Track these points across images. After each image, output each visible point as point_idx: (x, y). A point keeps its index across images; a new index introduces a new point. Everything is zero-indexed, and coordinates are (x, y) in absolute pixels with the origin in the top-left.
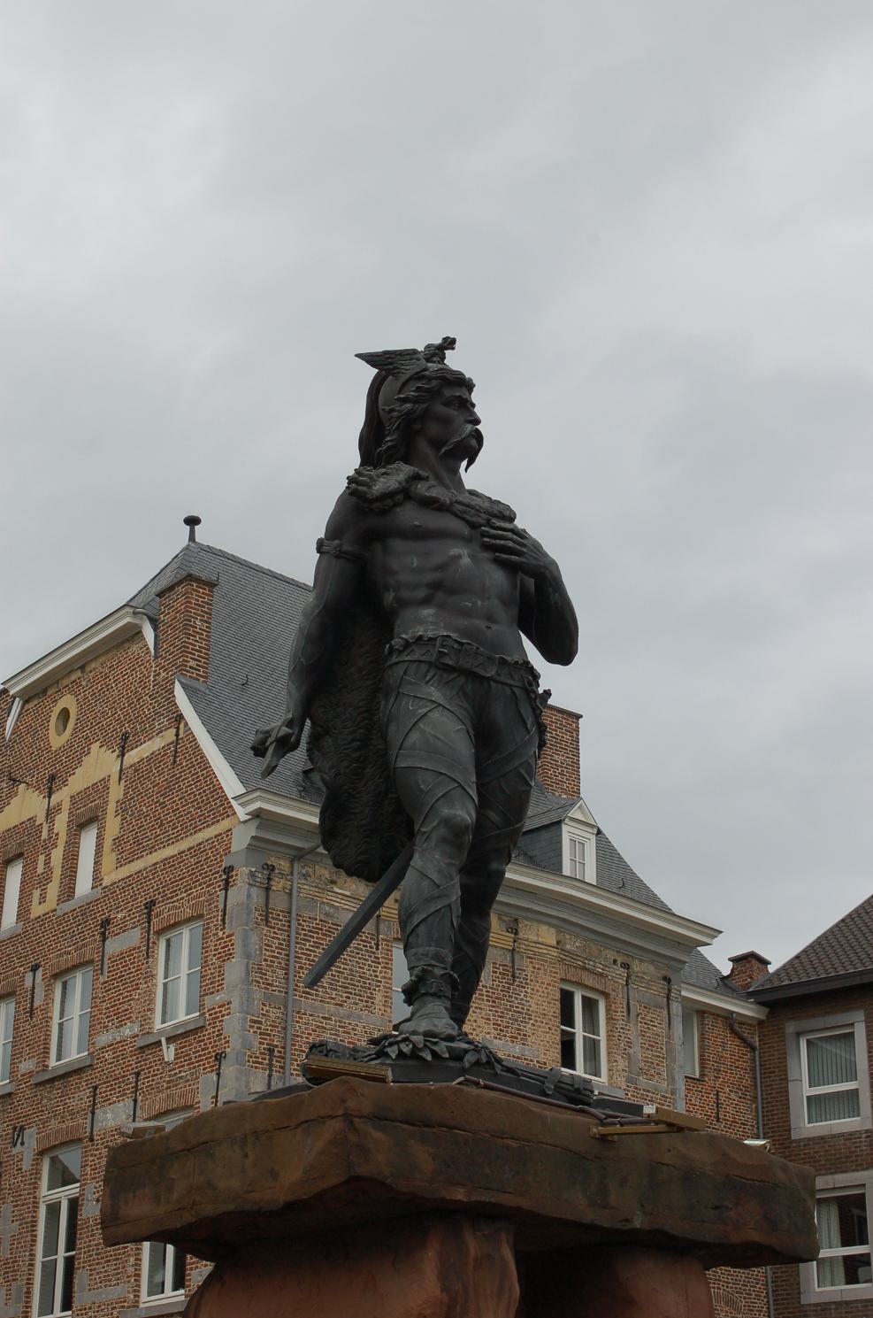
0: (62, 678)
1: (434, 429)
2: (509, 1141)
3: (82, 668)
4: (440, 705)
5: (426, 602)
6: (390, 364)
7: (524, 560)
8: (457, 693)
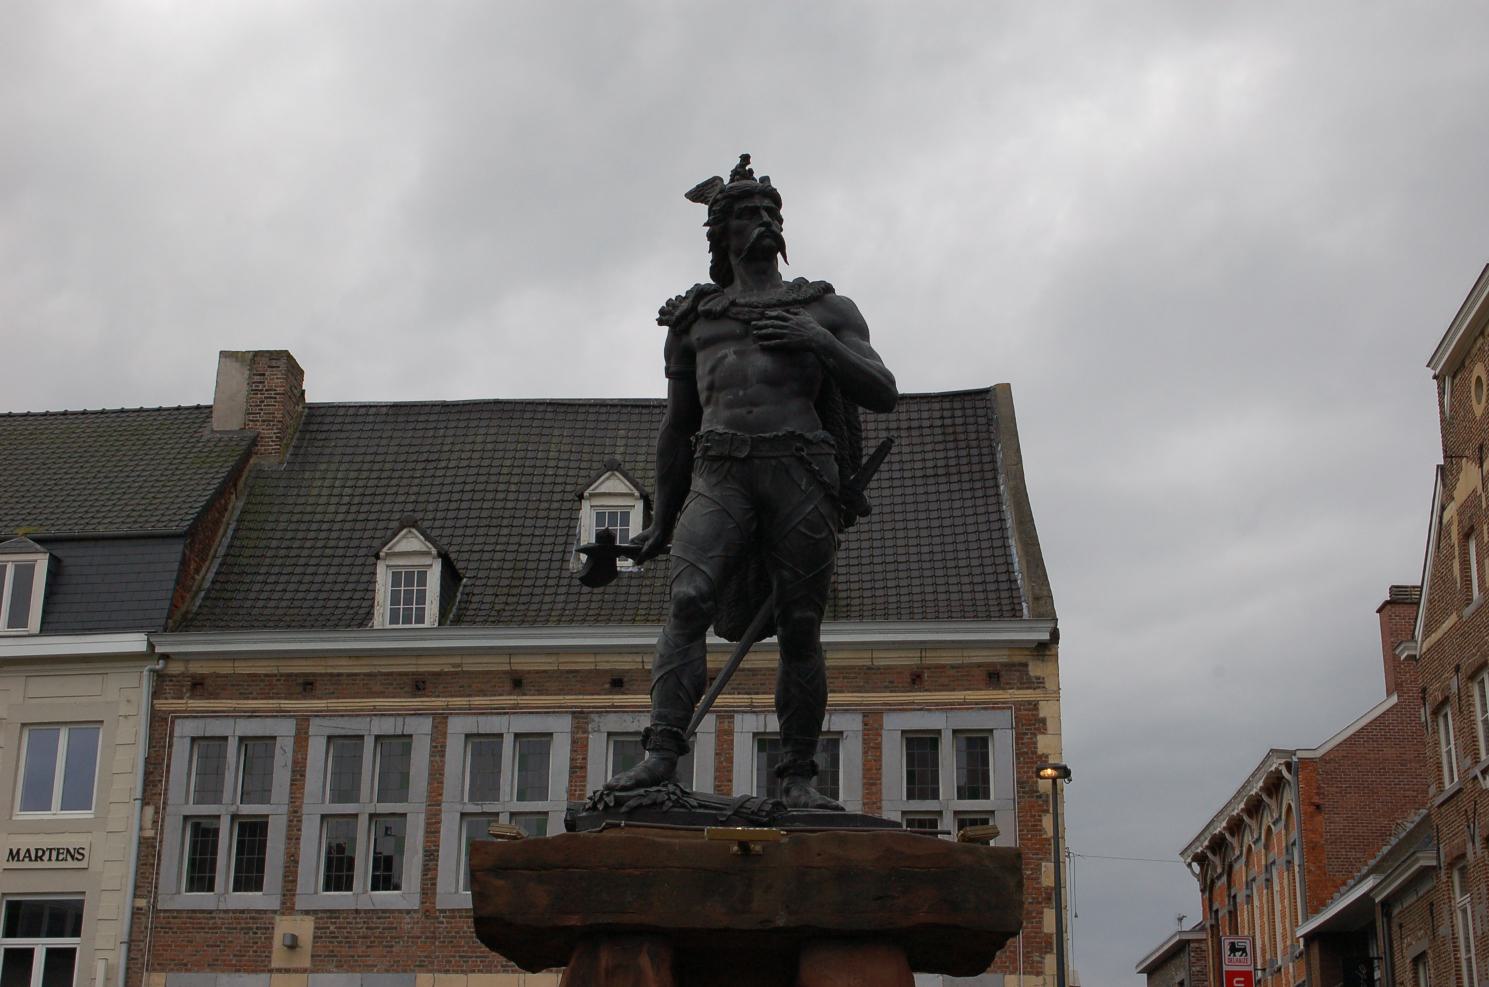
0: (1472, 347)
1: (734, 243)
2: (631, 870)
3: (1482, 333)
4: (700, 494)
5: (708, 401)
6: (702, 195)
7: (785, 340)
8: (725, 477)
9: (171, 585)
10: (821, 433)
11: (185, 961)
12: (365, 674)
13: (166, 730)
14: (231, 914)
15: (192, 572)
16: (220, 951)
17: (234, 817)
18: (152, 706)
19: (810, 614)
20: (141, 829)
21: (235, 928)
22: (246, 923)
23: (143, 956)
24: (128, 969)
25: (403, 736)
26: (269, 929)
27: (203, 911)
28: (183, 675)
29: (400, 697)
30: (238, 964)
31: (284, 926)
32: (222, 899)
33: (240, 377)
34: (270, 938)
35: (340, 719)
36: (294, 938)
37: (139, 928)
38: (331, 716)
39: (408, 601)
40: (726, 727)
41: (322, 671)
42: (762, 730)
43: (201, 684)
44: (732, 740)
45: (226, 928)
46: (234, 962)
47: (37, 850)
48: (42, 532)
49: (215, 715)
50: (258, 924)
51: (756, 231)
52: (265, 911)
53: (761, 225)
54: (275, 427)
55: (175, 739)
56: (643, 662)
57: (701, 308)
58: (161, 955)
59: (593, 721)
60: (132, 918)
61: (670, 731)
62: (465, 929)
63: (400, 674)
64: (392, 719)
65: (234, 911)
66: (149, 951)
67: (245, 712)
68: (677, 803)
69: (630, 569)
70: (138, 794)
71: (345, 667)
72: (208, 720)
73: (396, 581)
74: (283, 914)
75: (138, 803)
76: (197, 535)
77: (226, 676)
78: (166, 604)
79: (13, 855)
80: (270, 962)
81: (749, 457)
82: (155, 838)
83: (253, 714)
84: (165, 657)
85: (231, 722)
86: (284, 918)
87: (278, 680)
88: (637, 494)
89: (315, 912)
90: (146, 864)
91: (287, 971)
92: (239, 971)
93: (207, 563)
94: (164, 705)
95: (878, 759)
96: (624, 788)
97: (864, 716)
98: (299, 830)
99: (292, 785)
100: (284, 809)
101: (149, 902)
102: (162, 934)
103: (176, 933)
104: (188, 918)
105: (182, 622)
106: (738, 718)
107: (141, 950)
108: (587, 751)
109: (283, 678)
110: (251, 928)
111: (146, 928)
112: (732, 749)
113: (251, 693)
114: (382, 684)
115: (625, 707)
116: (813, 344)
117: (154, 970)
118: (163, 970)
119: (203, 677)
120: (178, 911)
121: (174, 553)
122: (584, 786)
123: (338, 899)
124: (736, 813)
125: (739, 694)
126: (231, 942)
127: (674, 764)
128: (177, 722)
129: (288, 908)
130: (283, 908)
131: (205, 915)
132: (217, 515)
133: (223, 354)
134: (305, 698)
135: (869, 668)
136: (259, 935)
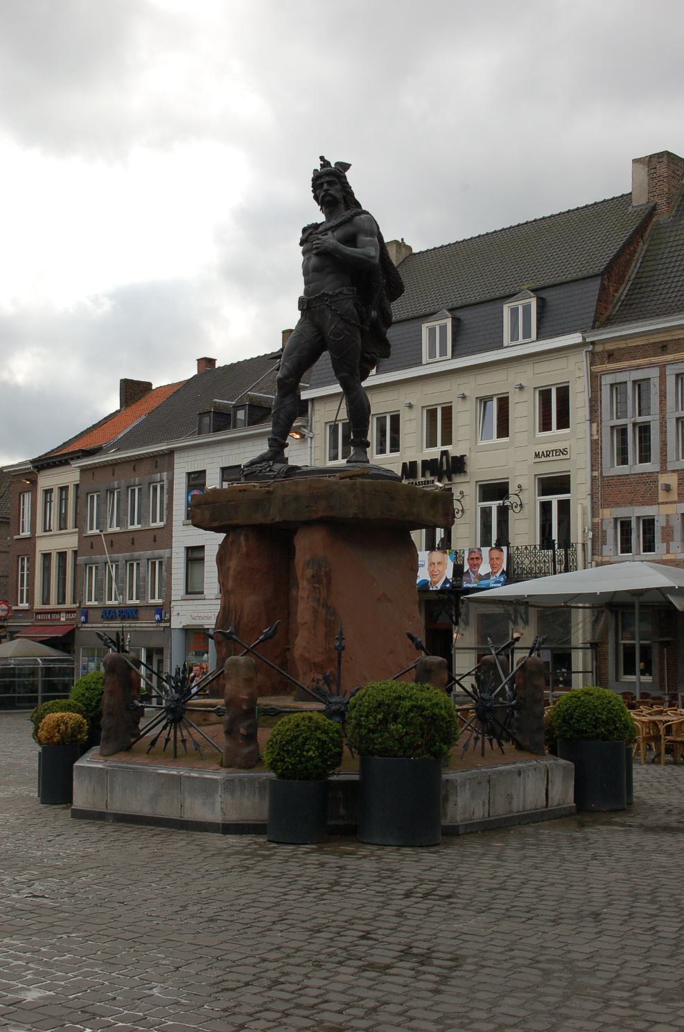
9: (595, 303)
15: (612, 293)
17: (634, 424)
20: (591, 435)
24: (592, 508)
27: (624, 475)
28: (603, 351)
33: (643, 171)
41: (670, 338)
47: (547, 451)
48: (534, 286)
49: (621, 370)
50: (650, 478)
52: (653, 473)
55: (603, 386)
60: (592, 484)
65: (639, 474)
70: (588, 418)
74: (662, 473)
75: (588, 422)
76: (613, 271)
77: (623, 349)
79: (537, 455)
83: (638, 368)
84: (593, 343)
85: (628, 373)
86: (663, 475)
89: (677, 471)
90: (595, 454)
91: (667, 503)
92: (643, 505)
93: (624, 285)
98: (666, 427)
99: (660, 404)
100: (657, 417)
105: (602, 320)
118: (608, 508)
120: (613, 476)
121: (595, 285)
124: (278, 473)
128: (603, 377)
129: (664, 470)
132: (628, 257)
133: (635, 161)
134: (663, 355)
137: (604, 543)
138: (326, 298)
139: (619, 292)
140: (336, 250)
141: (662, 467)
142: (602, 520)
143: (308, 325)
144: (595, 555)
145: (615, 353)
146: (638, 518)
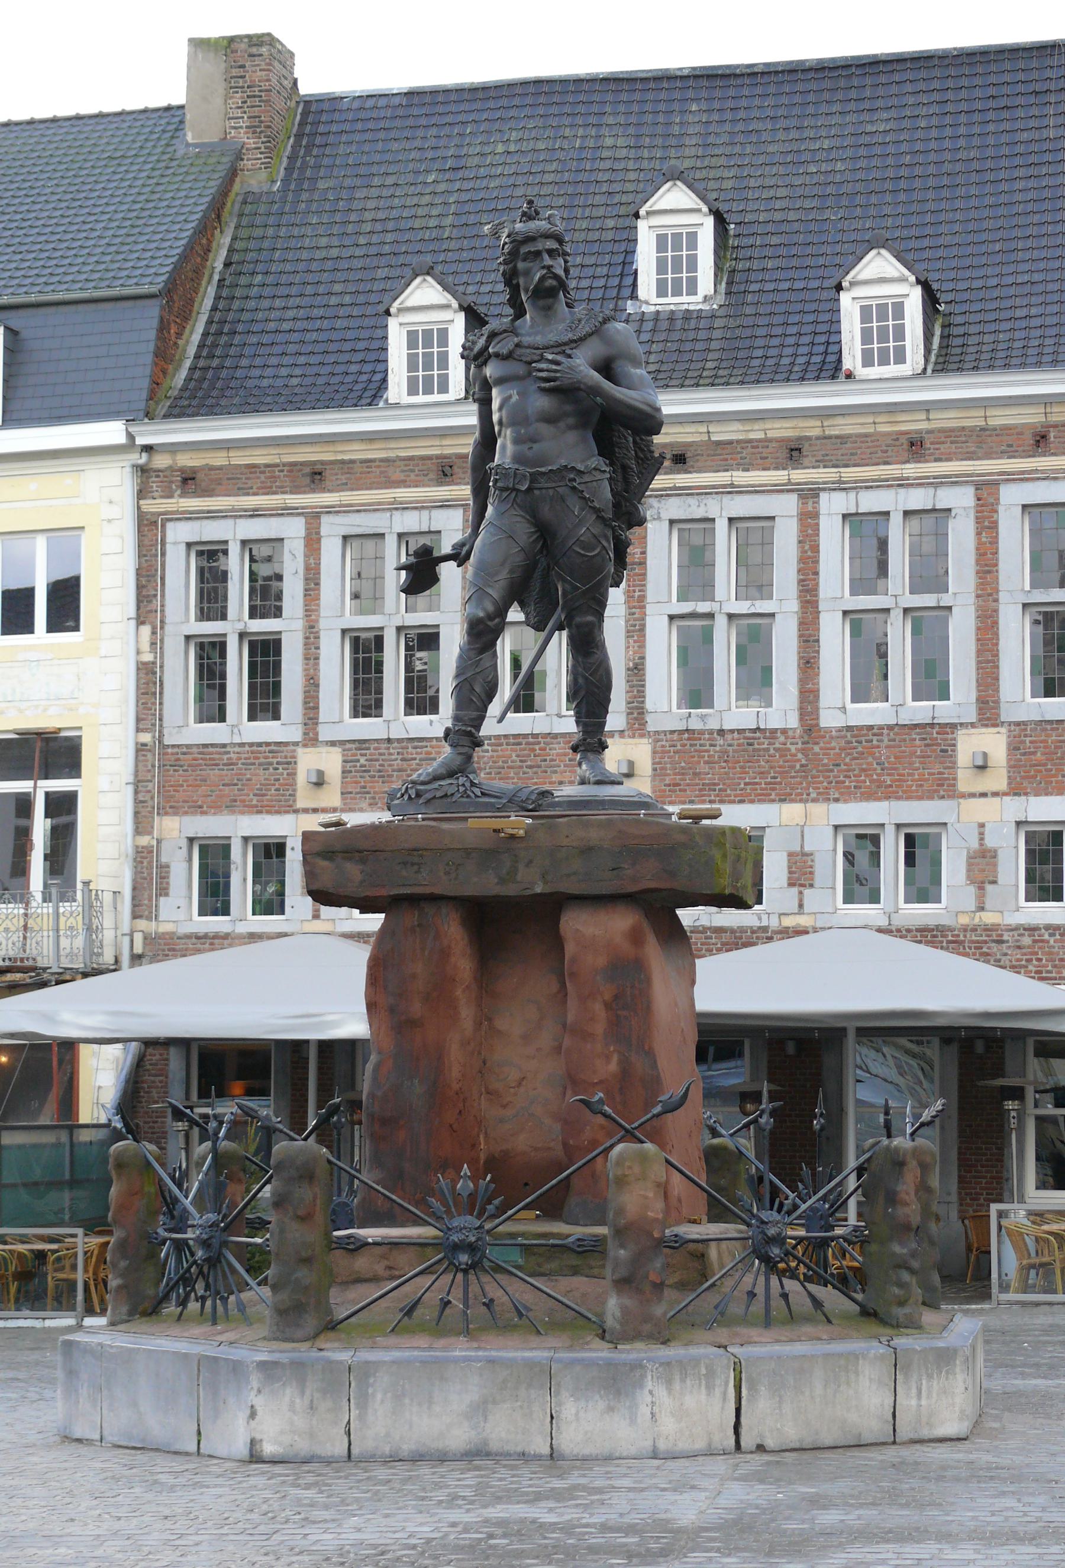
7: (558, 383)
9: (149, 359)
10: (597, 461)
11: (199, 803)
12: (382, 460)
13: (157, 535)
14: (247, 748)
16: (239, 790)
17: (242, 635)
18: (139, 508)
19: (590, 618)
20: (138, 652)
21: (254, 764)
22: (266, 758)
23: (152, 798)
24: (136, 814)
25: (430, 532)
26: (291, 763)
28: (170, 468)
29: (424, 486)
30: (259, 804)
31: (308, 761)
32: (236, 730)
33: (215, 67)
34: (293, 775)
35: (356, 515)
36: (320, 774)
37: (146, 766)
38: (345, 512)
39: (428, 366)
40: (810, 509)
42: (853, 511)
43: (194, 479)
44: (818, 524)
45: (243, 764)
46: (254, 802)
49: (211, 515)
51: (538, 276)
52: (286, 744)
53: (543, 267)
54: (262, 135)
55: (168, 546)
56: (709, 432)
57: (491, 350)
58: (172, 796)
59: (651, 507)
61: (464, 731)
62: (514, 758)
63: (423, 458)
64: (416, 513)
65: (251, 745)
66: (159, 792)
67: (246, 511)
68: (465, 795)
69: (698, 307)
70: (132, 613)
71: (357, 452)
72: (205, 522)
73: (412, 343)
74: (305, 746)
75: (133, 623)
78: (145, 383)
80: (295, 801)
81: (529, 489)
82: (154, 663)
83: (255, 513)
84: (148, 449)
85: (230, 522)
87: (282, 471)
88: (705, 209)
89: (342, 743)
90: (147, 694)
92: (259, 812)
94: (150, 506)
95: (995, 541)
96: (423, 783)
97: (977, 489)
98: (318, 648)
99: (305, 595)
100: (299, 625)
101: (154, 737)
102: (171, 772)
103: (186, 771)
104: (200, 753)
106: (824, 497)
107: (149, 791)
108: (646, 543)
109: (286, 468)
110: (271, 764)
111: (153, 766)
112: (818, 535)
113: (252, 488)
114: (403, 471)
115: (689, 488)
116: (582, 386)
117: (166, 814)
118: (175, 814)
119: (194, 470)
120: (187, 746)
122: (644, 585)
123: (368, 728)
125: (825, 467)
126: (249, 780)
127: (469, 758)
128: (170, 526)
129: (311, 739)
130: (305, 739)
131: (218, 749)
134: (313, 491)
135: (983, 429)
136: (281, 770)
137: (163, 891)
138: (572, 476)
139: (184, 337)
140: (595, 391)
141: (305, 734)
142: (159, 842)
143: (519, 519)
144: (140, 917)
145: (200, 476)
146: (246, 839)
